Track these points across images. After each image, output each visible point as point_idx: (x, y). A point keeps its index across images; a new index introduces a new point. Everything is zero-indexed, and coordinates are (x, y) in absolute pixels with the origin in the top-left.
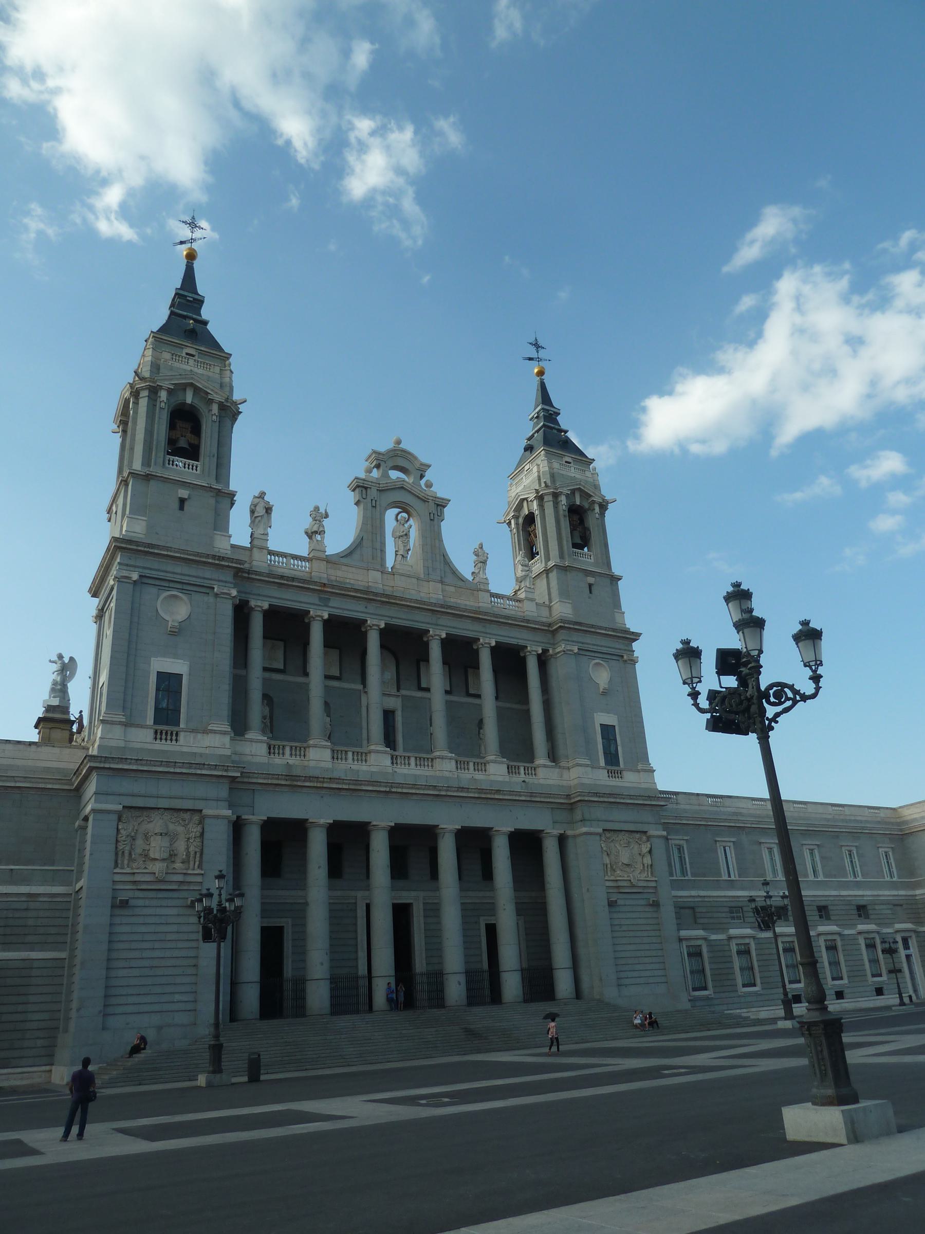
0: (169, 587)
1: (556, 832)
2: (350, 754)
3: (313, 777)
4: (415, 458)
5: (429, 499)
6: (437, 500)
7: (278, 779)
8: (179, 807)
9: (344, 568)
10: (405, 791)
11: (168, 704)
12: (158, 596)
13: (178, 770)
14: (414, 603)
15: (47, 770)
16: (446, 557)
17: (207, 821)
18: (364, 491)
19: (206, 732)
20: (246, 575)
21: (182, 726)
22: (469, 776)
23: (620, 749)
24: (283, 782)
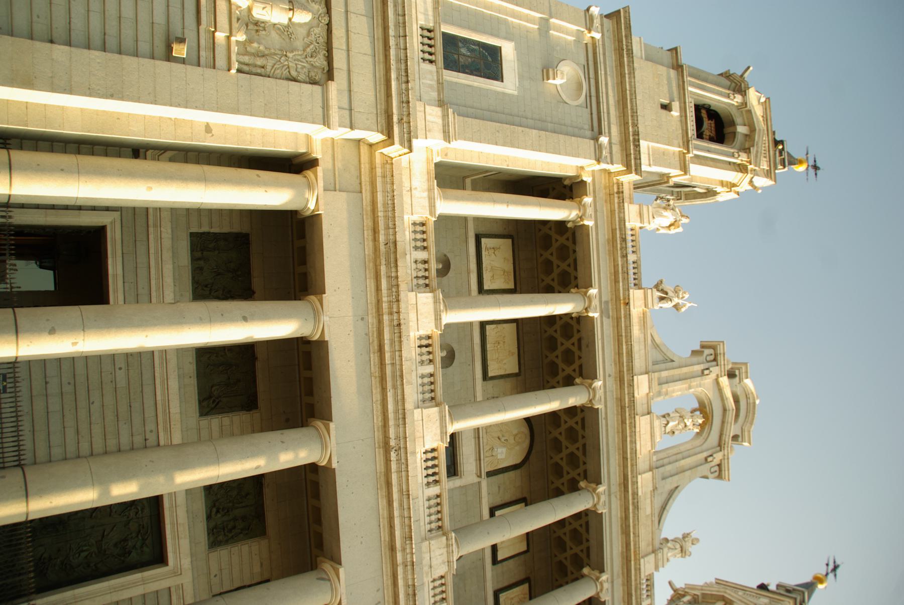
0: (589, 78)
2: (429, 369)
3: (398, 292)
4: (751, 424)
5: (724, 450)
6: (726, 461)
7: (387, 228)
11: (464, 55)
12: (577, 64)
13: (392, 42)
14: (632, 449)
16: (677, 491)
17: (317, 89)
18: (712, 358)
20: (616, 190)
24: (382, 238)
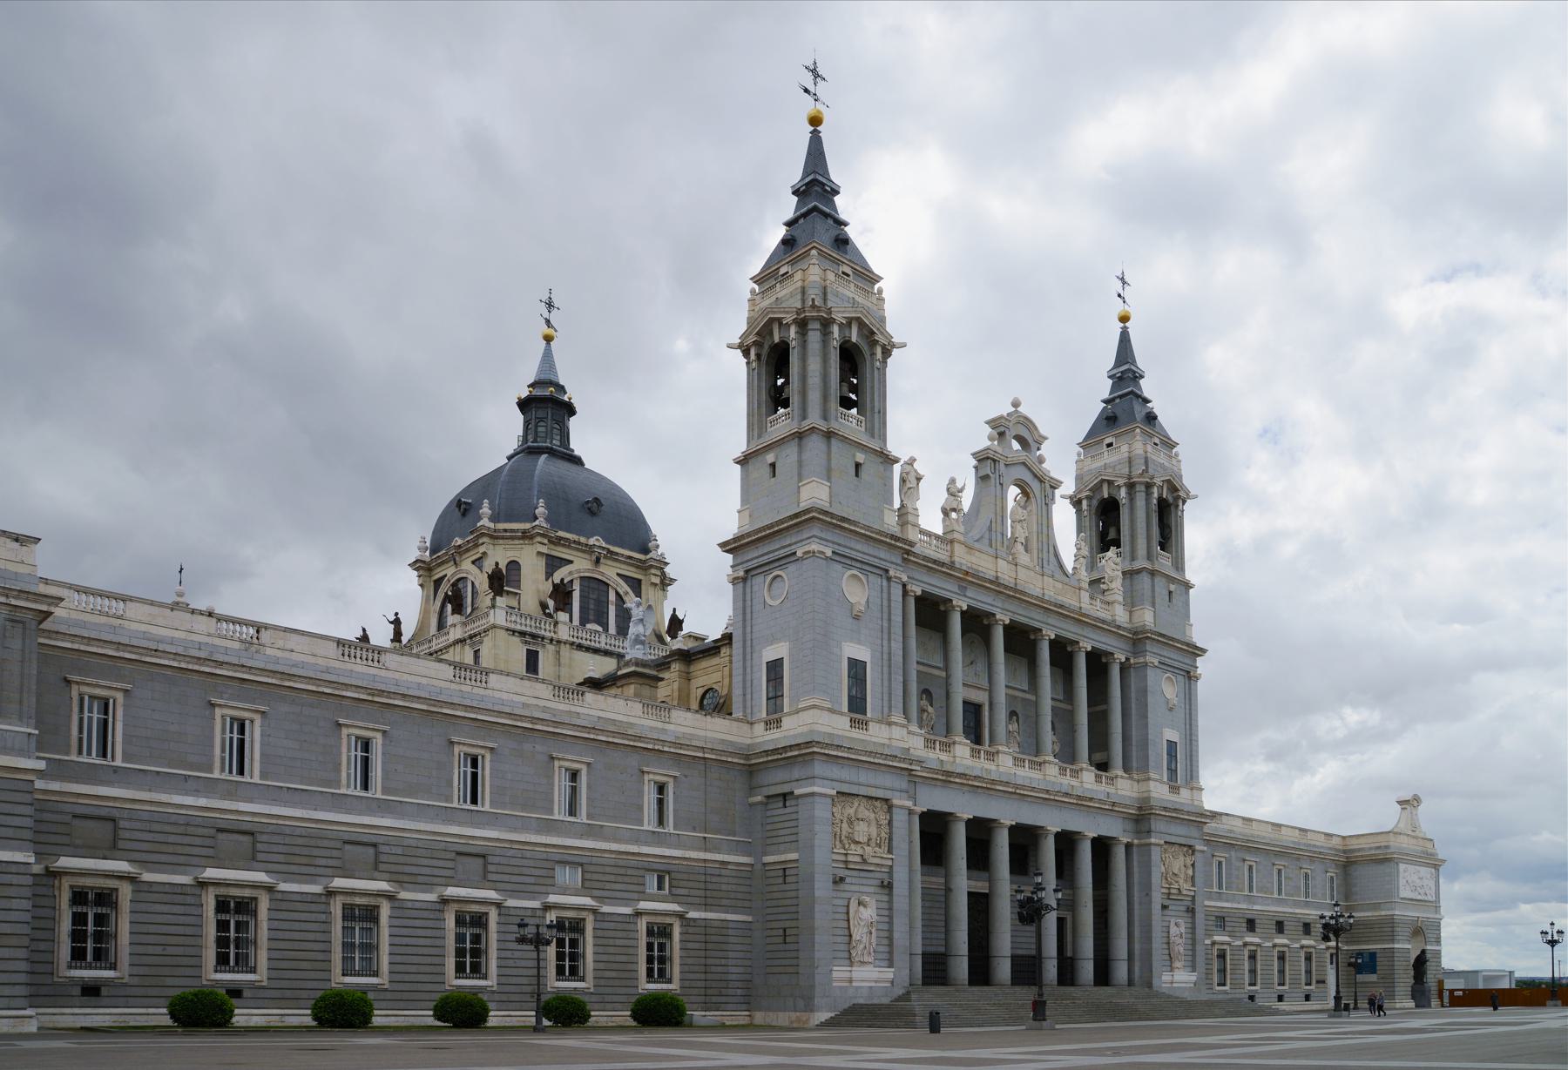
1: (1125, 840)
8: (874, 795)
9: (977, 553)
10: (1026, 793)
11: (856, 692)
12: (844, 574)
13: (876, 761)
14: (1035, 599)
15: (723, 741)
17: (894, 810)
19: (890, 724)
20: (906, 556)
21: (869, 715)
22: (1066, 782)
23: (1178, 764)
24: (940, 777)
